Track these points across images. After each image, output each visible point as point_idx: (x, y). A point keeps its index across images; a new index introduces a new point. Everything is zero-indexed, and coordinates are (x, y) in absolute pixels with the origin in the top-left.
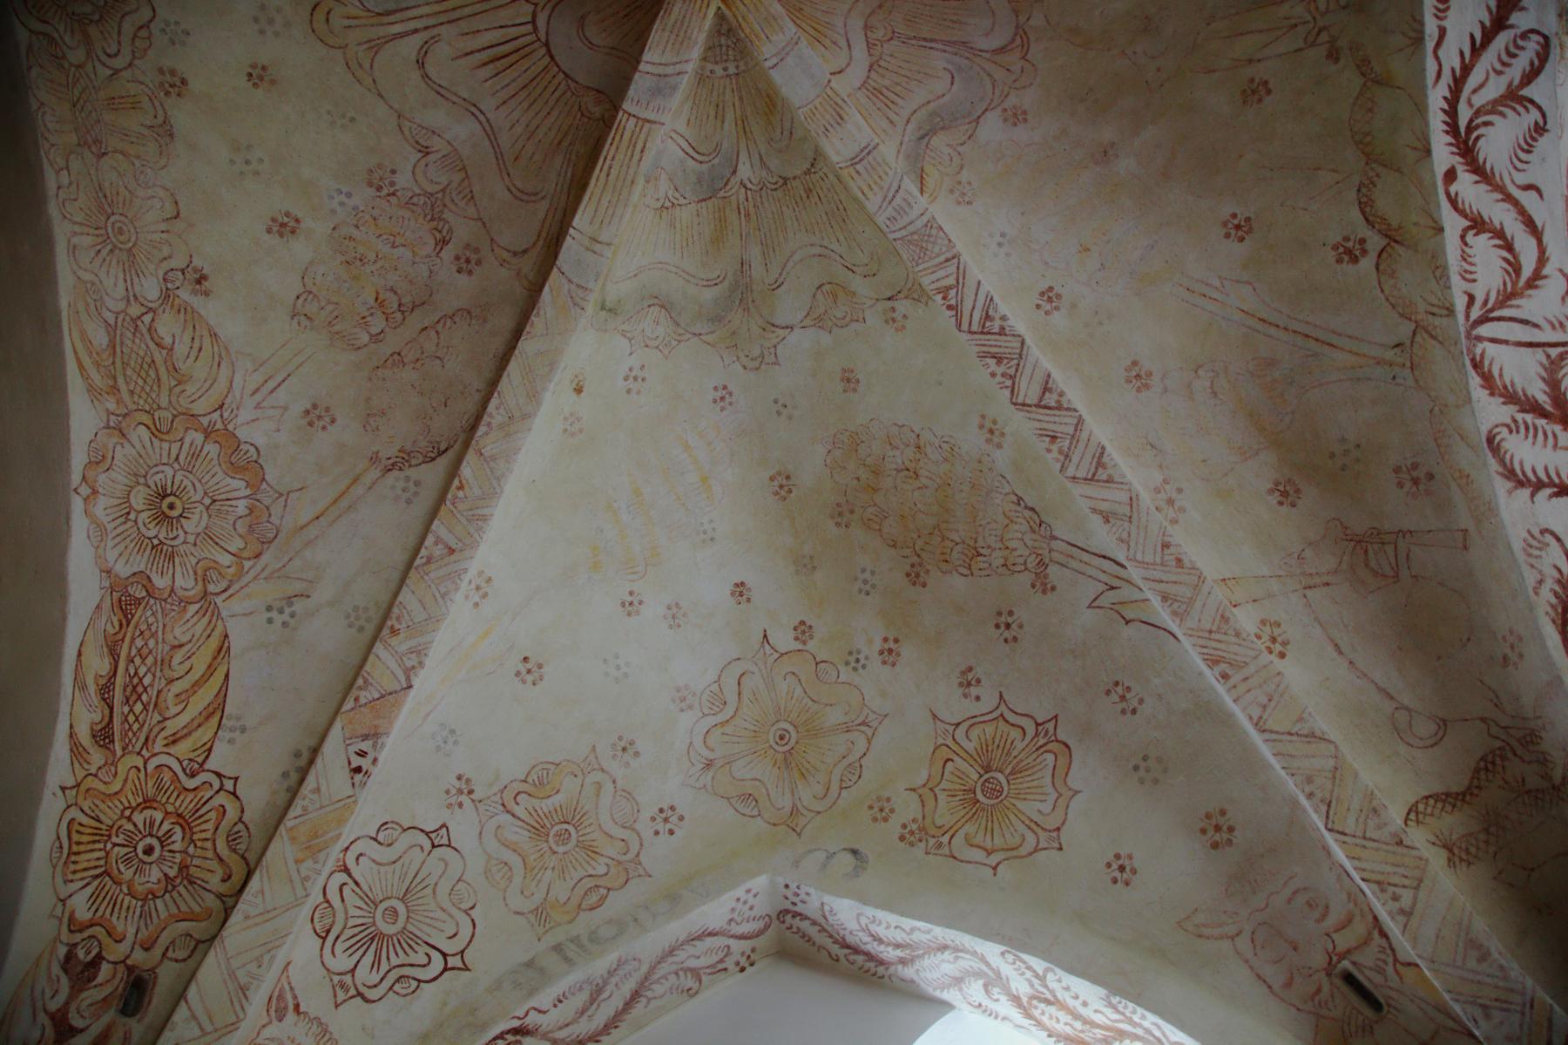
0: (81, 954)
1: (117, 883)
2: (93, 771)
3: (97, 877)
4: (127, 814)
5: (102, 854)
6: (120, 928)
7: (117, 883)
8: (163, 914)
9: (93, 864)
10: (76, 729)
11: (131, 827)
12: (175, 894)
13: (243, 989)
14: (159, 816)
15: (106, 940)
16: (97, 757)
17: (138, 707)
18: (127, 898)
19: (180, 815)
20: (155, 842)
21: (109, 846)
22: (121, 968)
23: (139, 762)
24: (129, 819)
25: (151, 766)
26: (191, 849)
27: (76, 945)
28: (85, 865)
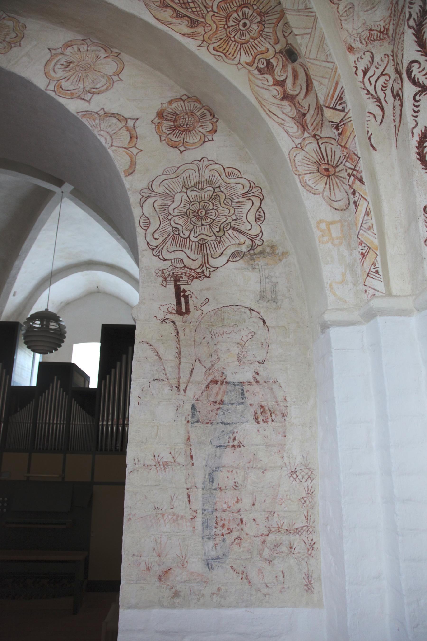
0: (262, 66)
1: (248, 42)
2: (204, 33)
3: (240, 49)
4: (226, 26)
6: (263, 49)
7: (248, 42)
8: (271, 30)
9: (235, 48)
10: (183, 32)
11: (232, 28)
12: (267, 22)
13: (307, 8)
14: (235, 15)
15: (264, 56)
16: (200, 29)
17: (192, 5)
18: (256, 41)
19: (240, 6)
20: (243, 21)
21: (233, 39)
22: (277, 55)
24: (229, 27)
25: (215, 9)
26: (255, 7)
27: (257, 67)
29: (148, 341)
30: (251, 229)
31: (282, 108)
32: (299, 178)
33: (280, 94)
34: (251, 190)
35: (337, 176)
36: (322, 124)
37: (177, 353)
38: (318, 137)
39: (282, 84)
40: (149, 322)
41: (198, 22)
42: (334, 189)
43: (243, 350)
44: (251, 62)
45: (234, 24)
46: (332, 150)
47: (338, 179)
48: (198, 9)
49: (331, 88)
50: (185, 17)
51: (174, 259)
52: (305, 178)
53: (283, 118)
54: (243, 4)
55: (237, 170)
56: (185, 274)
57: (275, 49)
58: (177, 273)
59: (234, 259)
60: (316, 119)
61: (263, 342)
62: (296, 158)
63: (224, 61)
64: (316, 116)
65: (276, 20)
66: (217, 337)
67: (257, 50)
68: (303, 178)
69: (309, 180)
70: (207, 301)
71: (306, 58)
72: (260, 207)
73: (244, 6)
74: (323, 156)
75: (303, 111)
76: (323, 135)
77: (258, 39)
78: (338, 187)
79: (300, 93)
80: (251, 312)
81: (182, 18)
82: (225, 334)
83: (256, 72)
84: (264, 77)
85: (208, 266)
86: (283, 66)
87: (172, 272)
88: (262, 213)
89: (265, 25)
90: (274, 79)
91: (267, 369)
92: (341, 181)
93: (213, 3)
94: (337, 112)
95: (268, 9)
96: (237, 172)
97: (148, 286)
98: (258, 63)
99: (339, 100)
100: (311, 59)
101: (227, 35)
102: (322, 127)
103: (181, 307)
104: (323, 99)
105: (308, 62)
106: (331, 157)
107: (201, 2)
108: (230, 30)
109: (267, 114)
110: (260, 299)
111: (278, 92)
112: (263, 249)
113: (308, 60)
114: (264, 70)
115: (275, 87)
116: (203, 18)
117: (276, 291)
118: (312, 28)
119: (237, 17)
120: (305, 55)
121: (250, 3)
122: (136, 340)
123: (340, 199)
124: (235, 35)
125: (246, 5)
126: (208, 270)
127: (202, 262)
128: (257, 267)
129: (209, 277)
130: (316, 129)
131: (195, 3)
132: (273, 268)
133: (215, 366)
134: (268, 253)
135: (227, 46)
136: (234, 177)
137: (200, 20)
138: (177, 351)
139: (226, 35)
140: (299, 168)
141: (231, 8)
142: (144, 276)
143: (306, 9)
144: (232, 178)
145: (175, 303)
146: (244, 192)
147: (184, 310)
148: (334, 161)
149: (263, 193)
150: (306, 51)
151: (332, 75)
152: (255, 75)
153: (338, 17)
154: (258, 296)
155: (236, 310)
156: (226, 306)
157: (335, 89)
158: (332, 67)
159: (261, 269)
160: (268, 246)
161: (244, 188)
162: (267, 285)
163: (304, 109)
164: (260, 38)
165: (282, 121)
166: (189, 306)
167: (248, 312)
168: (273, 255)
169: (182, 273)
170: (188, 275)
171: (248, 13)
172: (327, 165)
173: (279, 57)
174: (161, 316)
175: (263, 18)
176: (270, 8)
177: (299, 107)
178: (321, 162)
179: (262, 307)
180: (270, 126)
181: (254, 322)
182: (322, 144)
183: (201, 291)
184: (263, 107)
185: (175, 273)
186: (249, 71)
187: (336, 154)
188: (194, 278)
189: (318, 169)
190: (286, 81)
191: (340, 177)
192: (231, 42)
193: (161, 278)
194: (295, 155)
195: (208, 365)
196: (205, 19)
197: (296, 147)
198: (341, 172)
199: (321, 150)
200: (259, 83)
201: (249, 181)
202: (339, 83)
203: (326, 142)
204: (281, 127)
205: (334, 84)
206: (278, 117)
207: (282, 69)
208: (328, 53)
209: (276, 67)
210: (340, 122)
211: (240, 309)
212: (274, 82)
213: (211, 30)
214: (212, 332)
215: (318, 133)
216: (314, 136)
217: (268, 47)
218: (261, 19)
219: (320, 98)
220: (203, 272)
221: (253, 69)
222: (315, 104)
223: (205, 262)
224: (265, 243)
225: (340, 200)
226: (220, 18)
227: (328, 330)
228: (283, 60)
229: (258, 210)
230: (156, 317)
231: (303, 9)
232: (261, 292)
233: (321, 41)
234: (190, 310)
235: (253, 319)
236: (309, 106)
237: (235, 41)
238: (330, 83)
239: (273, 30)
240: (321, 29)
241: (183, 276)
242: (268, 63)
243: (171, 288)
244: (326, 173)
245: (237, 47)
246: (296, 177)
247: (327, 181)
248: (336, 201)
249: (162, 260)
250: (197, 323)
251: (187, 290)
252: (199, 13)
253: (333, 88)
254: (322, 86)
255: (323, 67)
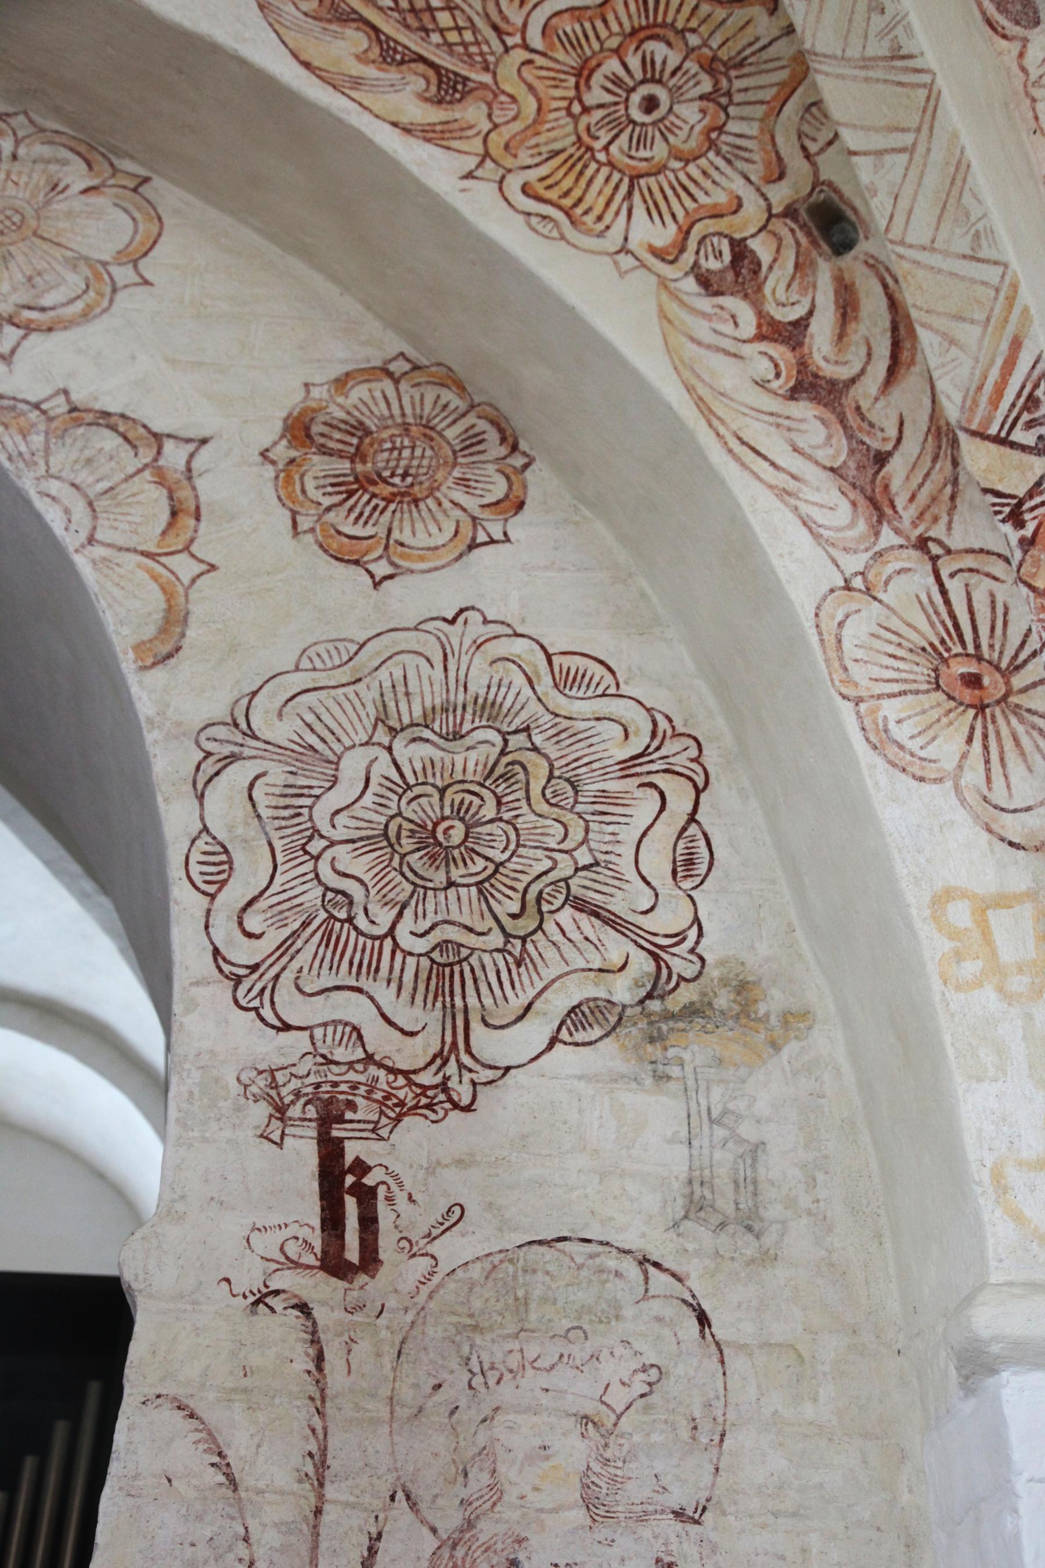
0: (713, 265)
1: (661, 169)
2: (486, 126)
3: (630, 194)
4: (577, 107)
5: (605, 171)
6: (720, 198)
7: (662, 169)
8: (753, 129)
9: (608, 190)
10: (404, 120)
11: (599, 114)
12: (738, 98)
13: (897, 55)
14: (613, 65)
15: (721, 225)
16: (473, 113)
17: (444, 19)
18: (692, 169)
19: (634, 32)
20: (644, 90)
21: (602, 157)
22: (779, 226)
23: (519, 55)
24: (586, 110)
25: (536, 41)
26: (693, 40)
27: (696, 264)
28: (602, 201)
29: (180, 1392)
30: (652, 909)
31: (789, 429)
32: (858, 713)
33: (784, 374)
34: (658, 749)
35: (1017, 706)
36: (953, 498)
37: (310, 1455)
38: (935, 549)
39: (792, 334)
40: (194, 1303)
41: (464, 85)
42: (1002, 759)
43: (608, 1454)
44: (673, 245)
45: (608, 98)
46: (993, 602)
47: (1022, 721)
48: (468, 36)
49: (991, 364)
50: (414, 61)
51: (325, 1025)
52: (881, 714)
53: (794, 471)
54: (648, 27)
55: (601, 662)
56: (369, 1092)
57: (766, 199)
58: (335, 1084)
59: (580, 1036)
60: (927, 475)
61: (697, 1414)
62: (847, 632)
63: (562, 237)
64: (929, 464)
65: (775, 90)
66: (492, 1382)
67: (695, 200)
68: (873, 711)
69: (899, 722)
70: (455, 1216)
71: (892, 242)
72: (692, 819)
73: (649, 32)
74: (957, 626)
75: (876, 444)
76: (956, 542)
77: (702, 162)
78: (1023, 754)
79: (863, 371)
80: (646, 1273)
81: (404, 67)
82: (530, 1372)
83: (690, 284)
84: (722, 308)
85: (466, 1059)
86: (797, 266)
87: (313, 1079)
88: (702, 843)
89: (732, 110)
90: (760, 314)
91: (714, 1549)
92: (1034, 727)
93: (528, 15)
94: (1016, 455)
95: (744, 49)
96: (599, 670)
97: (205, 1140)
98: (697, 253)
99: (1026, 408)
100: (911, 246)
101: (579, 138)
102: (953, 508)
103: (341, 1237)
104: (959, 403)
105: (901, 257)
106: (993, 628)
107: (480, 9)
108: (593, 121)
109: (730, 451)
110: (686, 1217)
111: (776, 366)
112: (704, 994)
113: (900, 250)
114: (722, 279)
115: (763, 346)
116: (486, 69)
117: (755, 1183)
118: (919, 130)
119: (621, 72)
120: (887, 230)
121: (672, 25)
122: (127, 1391)
123: (1031, 803)
124: (610, 143)
125: (657, 30)
126: (467, 1076)
127: (443, 1042)
128: (675, 1071)
129: (468, 1109)
130: (928, 516)
131: (457, 13)
132: (743, 1082)
133: (481, 1525)
134: (722, 1013)
135: (577, 180)
136: (589, 694)
137: (473, 76)
138: (313, 1447)
139: (573, 138)
140: (858, 672)
141: (598, 38)
142: (191, 1093)
143: (893, 58)
144: (581, 694)
145: (316, 1222)
146: (627, 756)
147: (352, 1254)
148: (1003, 645)
149: (704, 760)
150: (892, 217)
151: (997, 311)
152: (685, 298)
153: (1021, 88)
154: (680, 1201)
155: (579, 1260)
156: (540, 1243)
157: (1010, 364)
158: (995, 281)
159: (691, 1083)
160: (724, 982)
161: (627, 736)
162: (718, 1155)
163: (880, 434)
164: (711, 155)
165: (792, 482)
166: (376, 1233)
167: (632, 1270)
168: (744, 1021)
169: (355, 1086)
170: (378, 1095)
171: (664, 62)
172: (974, 661)
173: (784, 232)
174: (250, 1277)
175: (724, 83)
176: (750, 44)
177: (860, 429)
178: (948, 650)
179: (697, 1253)
180: (743, 499)
181: (659, 1319)
182: (952, 576)
183: (432, 1169)
184: (716, 423)
185: (326, 1088)
186: (663, 283)
187: (1010, 617)
188: (403, 1111)
189: (937, 678)
190: (807, 326)
191: (1029, 711)
192: (593, 166)
193: (263, 1104)
194: (840, 617)
195: (450, 1521)
196: (495, 74)
197: (848, 588)
198: (1031, 692)
199: (947, 602)
200: (702, 330)
201: (648, 710)
202: (1027, 344)
203: (971, 570)
204: (786, 504)
205: (1004, 346)
206: (773, 464)
207: (793, 278)
208: (980, 226)
209: (771, 268)
210: (1030, 495)
211: (598, 1255)
212: (759, 326)
213: (515, 118)
214: (474, 1361)
215: (938, 531)
216: (922, 544)
217: (740, 193)
218: (716, 83)
219: (948, 397)
220: (444, 1086)
221: (680, 274)
222: (926, 418)
223: (454, 1044)
224: (713, 972)
225: (1028, 809)
226: (552, 74)
227: (991, 1381)
228: (798, 244)
229: (684, 829)
230: (228, 1280)
231: (884, 58)
232: (690, 1182)
233: (954, 179)
234: (382, 1256)
235: (655, 1307)
236: (901, 424)
237: (610, 164)
238: (987, 338)
239: (762, 130)
240: (955, 135)
241: (360, 1101)
242: (740, 251)
243: (303, 1150)
244: (967, 695)
245: (617, 187)
246: (847, 707)
247: (972, 728)
248: (1015, 811)
249: (273, 1027)
250: (409, 1317)
251: (371, 1163)
252: (473, 49)
253: (999, 362)
254: (954, 351)
255: (962, 278)
